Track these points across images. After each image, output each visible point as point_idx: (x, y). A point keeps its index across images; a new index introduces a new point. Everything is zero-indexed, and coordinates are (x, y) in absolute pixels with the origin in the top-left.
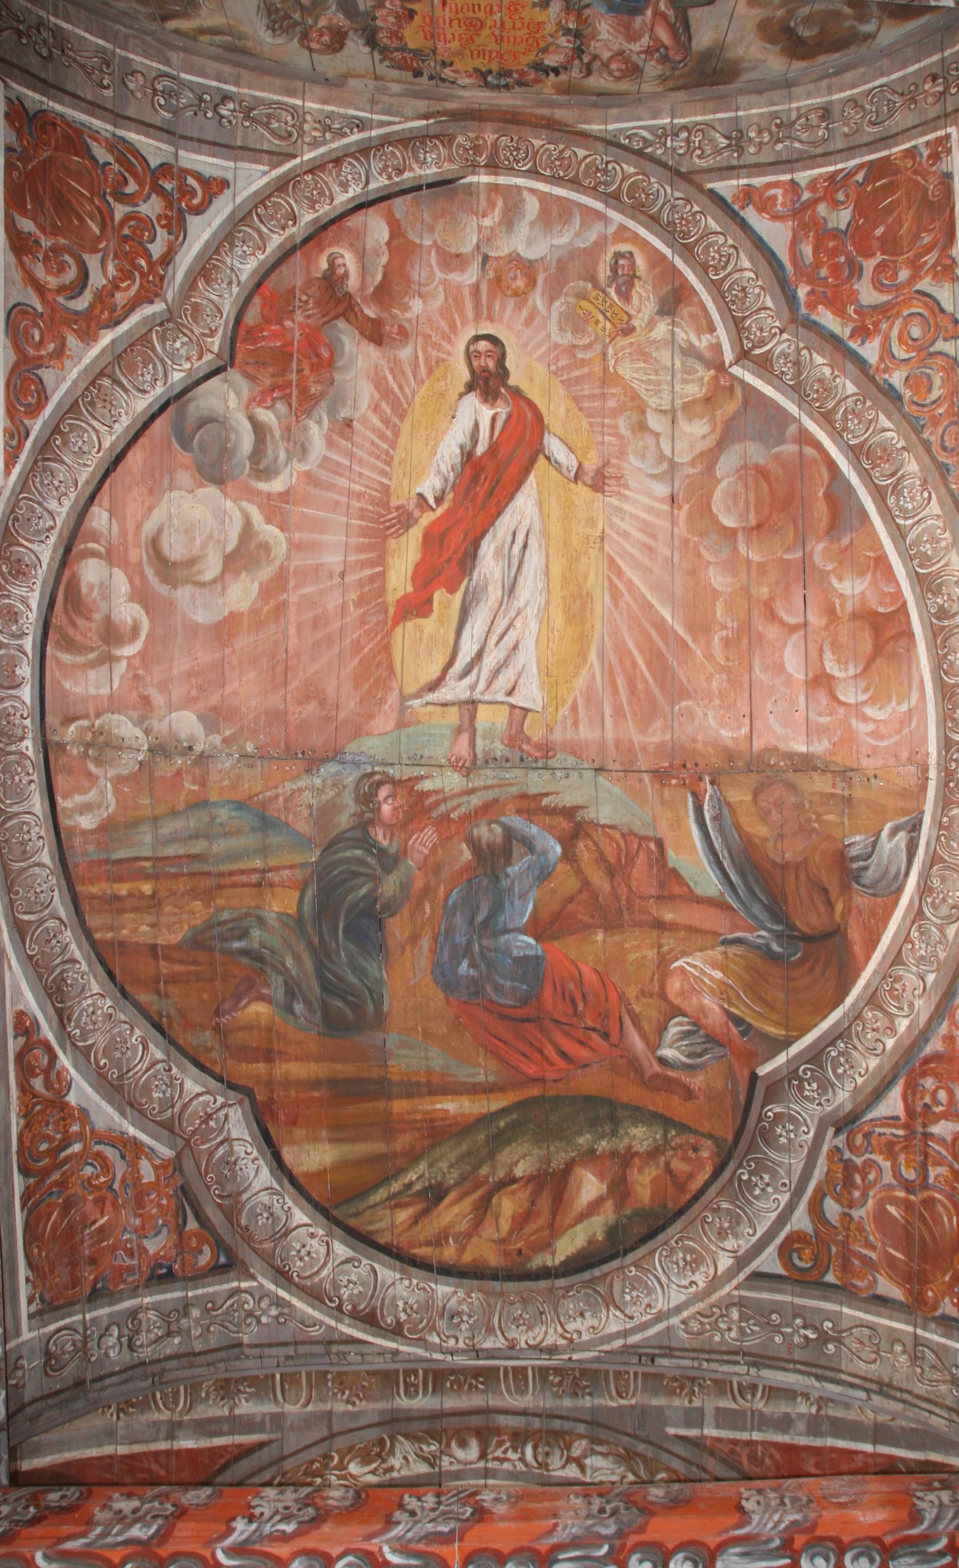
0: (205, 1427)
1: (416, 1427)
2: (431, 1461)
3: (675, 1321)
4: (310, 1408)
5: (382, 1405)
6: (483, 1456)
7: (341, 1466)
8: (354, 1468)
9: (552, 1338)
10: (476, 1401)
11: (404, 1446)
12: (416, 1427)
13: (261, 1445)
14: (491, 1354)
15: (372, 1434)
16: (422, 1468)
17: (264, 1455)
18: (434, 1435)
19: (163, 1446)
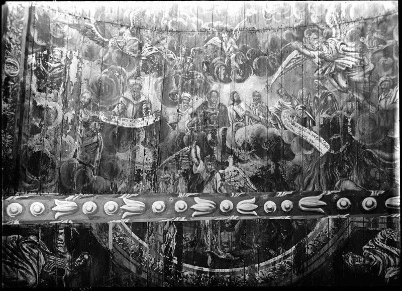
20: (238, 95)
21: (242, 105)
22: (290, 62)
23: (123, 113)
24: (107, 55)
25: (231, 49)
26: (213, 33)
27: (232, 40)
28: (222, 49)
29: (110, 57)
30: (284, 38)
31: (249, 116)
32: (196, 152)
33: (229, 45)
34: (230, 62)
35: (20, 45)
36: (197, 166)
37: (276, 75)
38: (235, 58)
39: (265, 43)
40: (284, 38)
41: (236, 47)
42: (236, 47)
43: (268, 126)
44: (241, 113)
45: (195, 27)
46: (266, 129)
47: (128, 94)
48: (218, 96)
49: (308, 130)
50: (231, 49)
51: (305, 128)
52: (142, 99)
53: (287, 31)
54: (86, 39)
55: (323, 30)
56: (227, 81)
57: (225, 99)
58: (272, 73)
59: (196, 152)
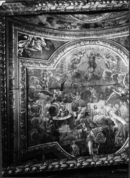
0: (63, 39)
1: (83, 40)
2: (85, 43)
3: (107, 17)
4: (73, 38)
5: (80, 38)
6: (89, 43)
7: (76, 44)
8: (77, 44)
9: (95, 20)
10: (89, 37)
11: (82, 42)
12: (83, 40)
13: (68, 42)
14: (90, 22)
15: (79, 41)
16: (84, 44)
17: (68, 43)
18: (85, 41)
19: (59, 40)
20: (96, 106)
21: (98, 109)
22: (112, 96)
23: (60, 116)
24: (53, 99)
25: (93, 92)
26: (87, 87)
27: (93, 89)
28: (90, 92)
29: (54, 100)
30: (110, 88)
31: (100, 113)
32: (84, 125)
33: (92, 91)
34: (93, 96)
35: (25, 103)
36: (85, 129)
37: (108, 100)
38: (95, 95)
39: (104, 90)
40: (110, 88)
41: (94, 91)
42: (94, 91)
43: (106, 116)
44: (98, 112)
45: (81, 86)
46: (105, 116)
47: (61, 110)
48: (90, 107)
49: (119, 117)
50: (93, 92)
51: (118, 116)
52: (66, 110)
53: (111, 86)
54: (47, 95)
55: (122, 86)
56: (92, 102)
57: (92, 108)
58: (106, 99)
59: (84, 125)
